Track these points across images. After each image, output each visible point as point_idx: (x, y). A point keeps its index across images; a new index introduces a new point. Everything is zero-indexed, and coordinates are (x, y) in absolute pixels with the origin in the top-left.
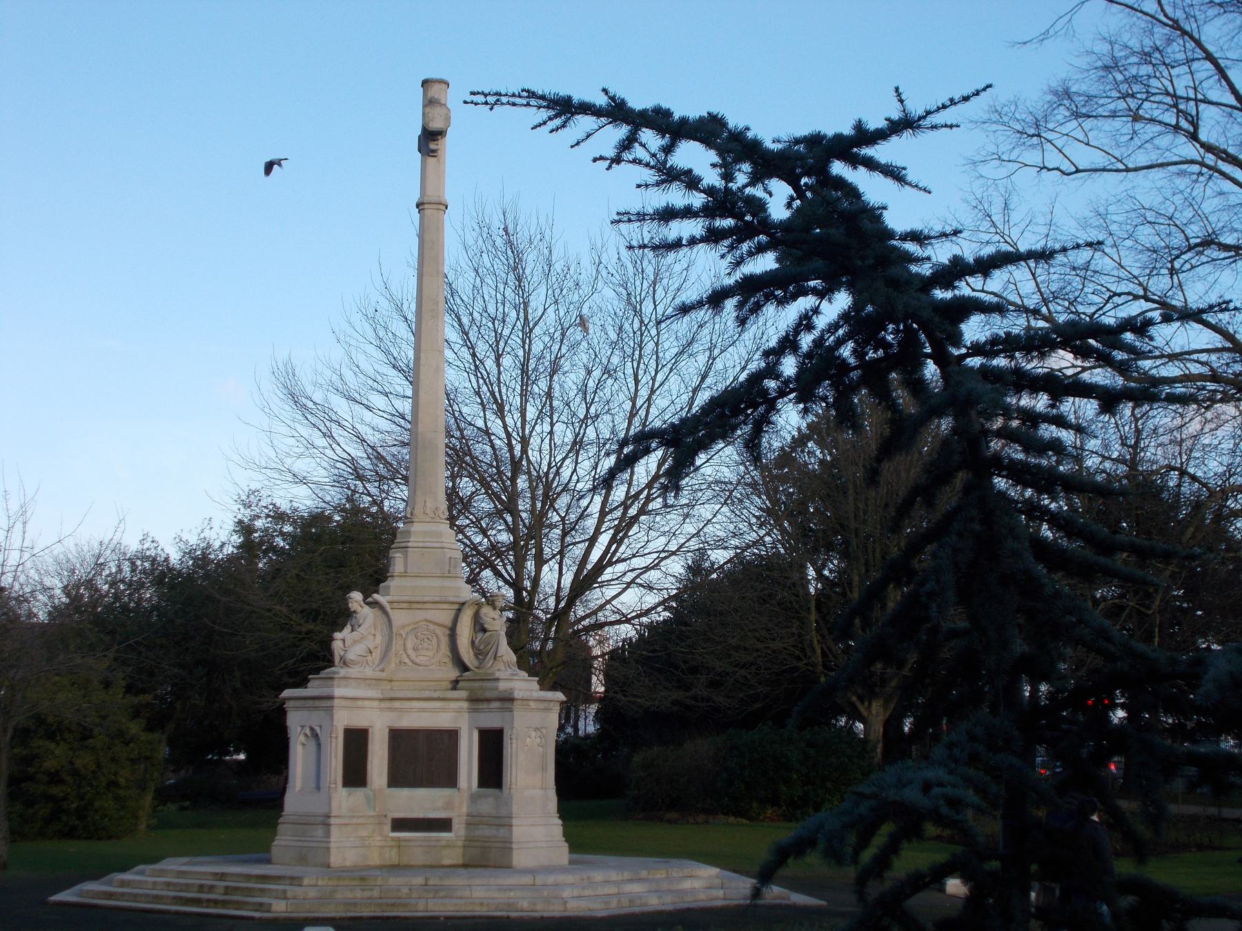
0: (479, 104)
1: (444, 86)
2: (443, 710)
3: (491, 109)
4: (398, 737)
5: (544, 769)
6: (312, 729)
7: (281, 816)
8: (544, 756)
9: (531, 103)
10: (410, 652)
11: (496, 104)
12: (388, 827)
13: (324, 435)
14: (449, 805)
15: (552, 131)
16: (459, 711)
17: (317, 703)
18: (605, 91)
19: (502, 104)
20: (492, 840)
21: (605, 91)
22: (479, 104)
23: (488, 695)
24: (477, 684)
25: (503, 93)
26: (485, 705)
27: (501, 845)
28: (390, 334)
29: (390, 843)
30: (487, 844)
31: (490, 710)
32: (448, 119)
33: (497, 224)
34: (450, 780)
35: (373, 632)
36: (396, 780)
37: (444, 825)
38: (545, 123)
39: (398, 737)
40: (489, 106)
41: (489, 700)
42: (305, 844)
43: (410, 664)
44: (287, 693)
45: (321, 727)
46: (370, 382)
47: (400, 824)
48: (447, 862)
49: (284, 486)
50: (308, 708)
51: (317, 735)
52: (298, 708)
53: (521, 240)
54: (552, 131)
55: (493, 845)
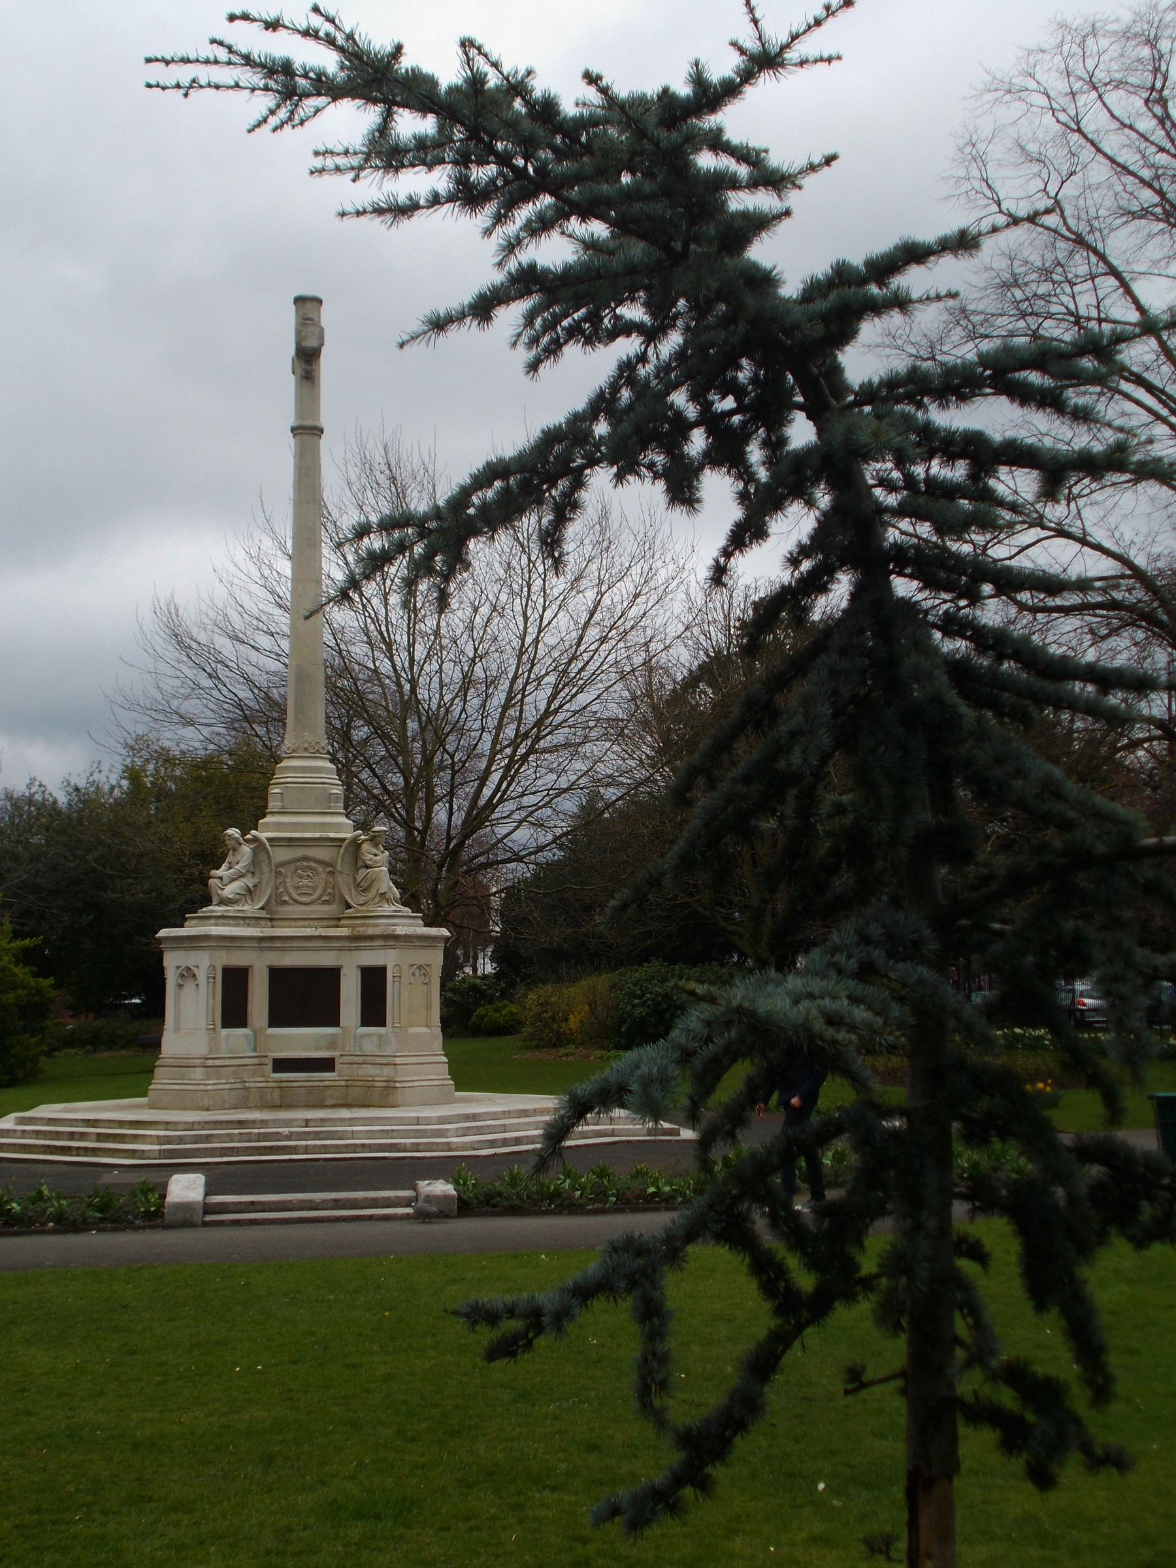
0: (168, 88)
1: (316, 304)
3: (186, 95)
4: (278, 975)
5: (429, 1007)
7: (159, 1059)
8: (428, 995)
9: (241, 84)
10: (291, 890)
11: (191, 87)
12: (270, 1067)
13: (210, 676)
14: (332, 1043)
15: (275, 130)
16: (339, 949)
19: (201, 87)
20: (376, 1079)
22: (168, 88)
25: (192, 57)
27: (384, 1084)
28: (275, 573)
30: (370, 1084)
31: (373, 948)
32: (321, 337)
33: (379, 458)
34: (334, 1021)
35: (252, 869)
36: (278, 1018)
37: (327, 1065)
38: (265, 120)
39: (278, 975)
40: (182, 91)
42: (183, 1087)
43: (291, 902)
44: (163, 933)
45: (197, 967)
46: (255, 622)
47: (281, 1065)
49: (172, 728)
50: (187, 949)
52: (174, 949)
53: (403, 476)
54: (275, 130)
55: (377, 1084)
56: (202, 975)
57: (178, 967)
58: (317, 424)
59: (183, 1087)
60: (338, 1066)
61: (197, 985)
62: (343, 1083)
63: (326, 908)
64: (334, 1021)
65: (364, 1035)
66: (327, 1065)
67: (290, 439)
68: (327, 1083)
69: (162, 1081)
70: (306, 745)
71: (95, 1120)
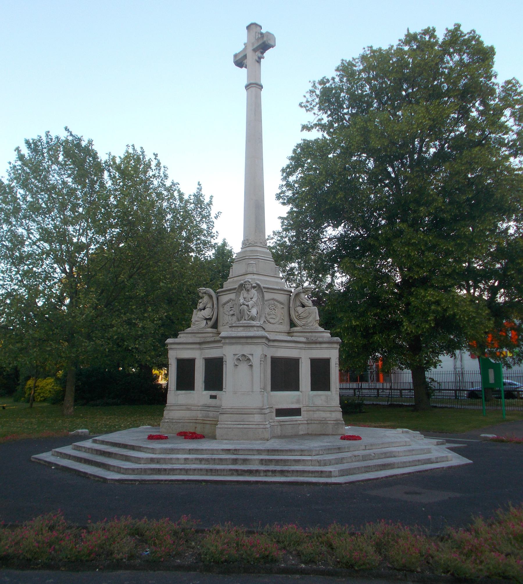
2: (295, 348)
6: (243, 355)
12: (274, 414)
16: (300, 348)
17: (249, 341)
18: (66, 129)
20: (327, 419)
21: (66, 129)
23: (320, 340)
24: (307, 334)
26: (318, 346)
27: (335, 422)
29: (276, 424)
31: (321, 348)
34: (296, 388)
41: (321, 343)
42: (245, 426)
45: (252, 355)
47: (280, 412)
48: (301, 433)
50: (242, 344)
51: (249, 359)
55: (329, 422)
56: (256, 361)
57: (235, 355)
58: (259, 83)
59: (245, 426)
60: (302, 413)
61: (251, 366)
62: (305, 422)
63: (281, 326)
64: (296, 388)
65: (315, 396)
66: (297, 412)
67: (263, 82)
68: (299, 422)
69: (226, 423)
70: (261, 241)
71: (235, 450)
